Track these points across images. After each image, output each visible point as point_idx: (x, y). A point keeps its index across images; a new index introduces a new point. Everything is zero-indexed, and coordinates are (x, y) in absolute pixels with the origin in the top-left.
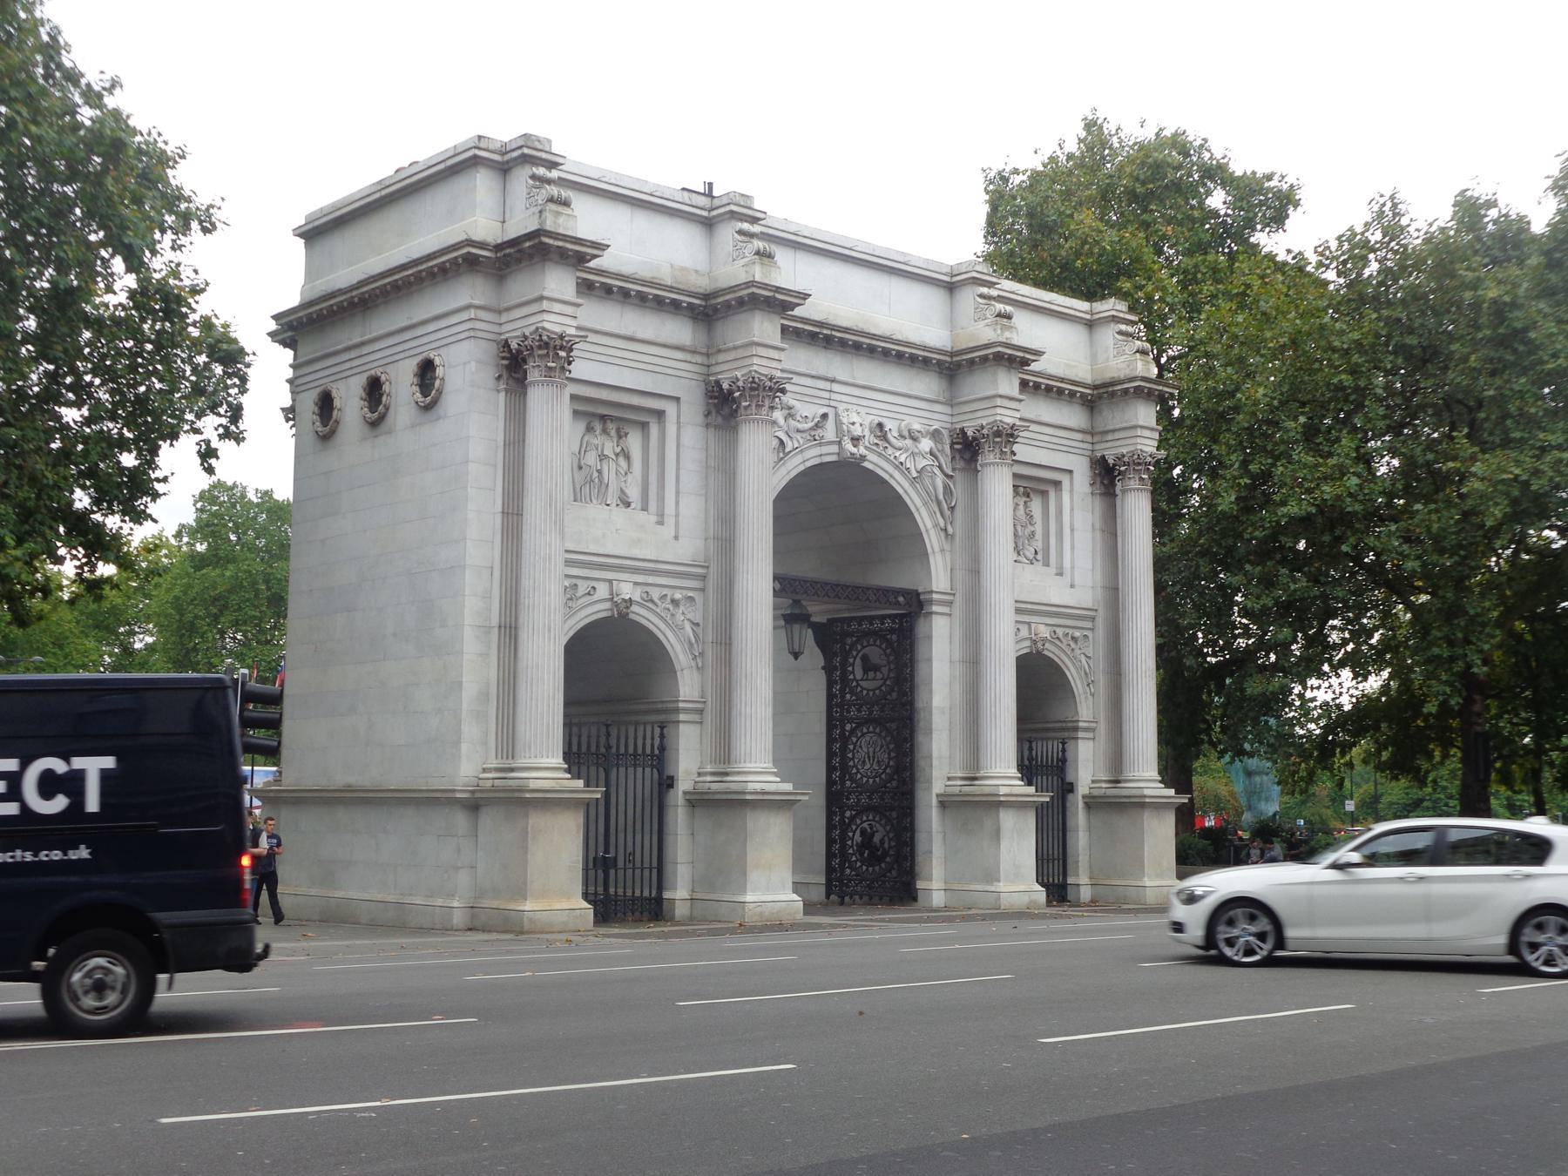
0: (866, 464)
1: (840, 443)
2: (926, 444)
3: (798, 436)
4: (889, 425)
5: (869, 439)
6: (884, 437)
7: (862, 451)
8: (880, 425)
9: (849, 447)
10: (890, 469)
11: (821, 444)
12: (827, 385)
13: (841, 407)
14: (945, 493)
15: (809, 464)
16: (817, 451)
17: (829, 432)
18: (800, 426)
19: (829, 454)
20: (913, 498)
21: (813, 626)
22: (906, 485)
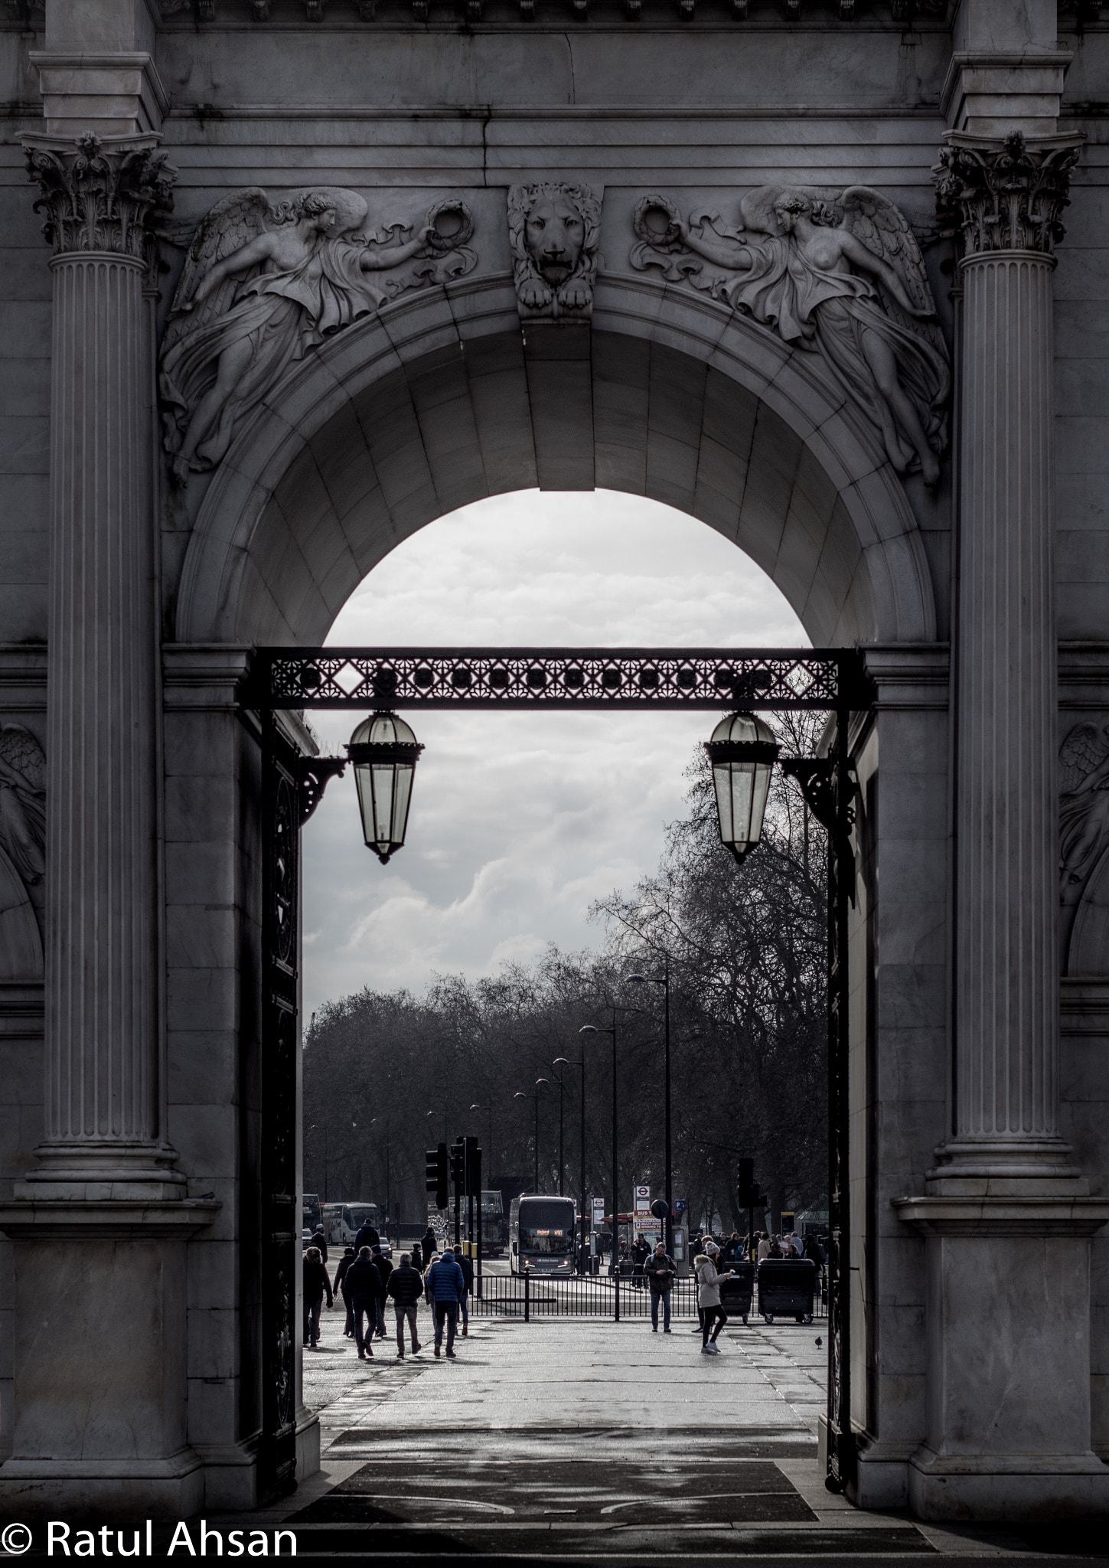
0: (605, 323)
1: (509, 281)
2: (823, 243)
3: (377, 287)
4: (687, 207)
5: (621, 251)
6: (676, 241)
7: (576, 290)
8: (656, 210)
9: (535, 290)
10: (711, 328)
11: (447, 295)
12: (472, 131)
13: (516, 183)
14: (901, 373)
15: (410, 352)
16: (441, 312)
17: (484, 256)
18: (370, 257)
19: (487, 314)
20: (797, 397)
21: (794, 767)
22: (771, 364)
